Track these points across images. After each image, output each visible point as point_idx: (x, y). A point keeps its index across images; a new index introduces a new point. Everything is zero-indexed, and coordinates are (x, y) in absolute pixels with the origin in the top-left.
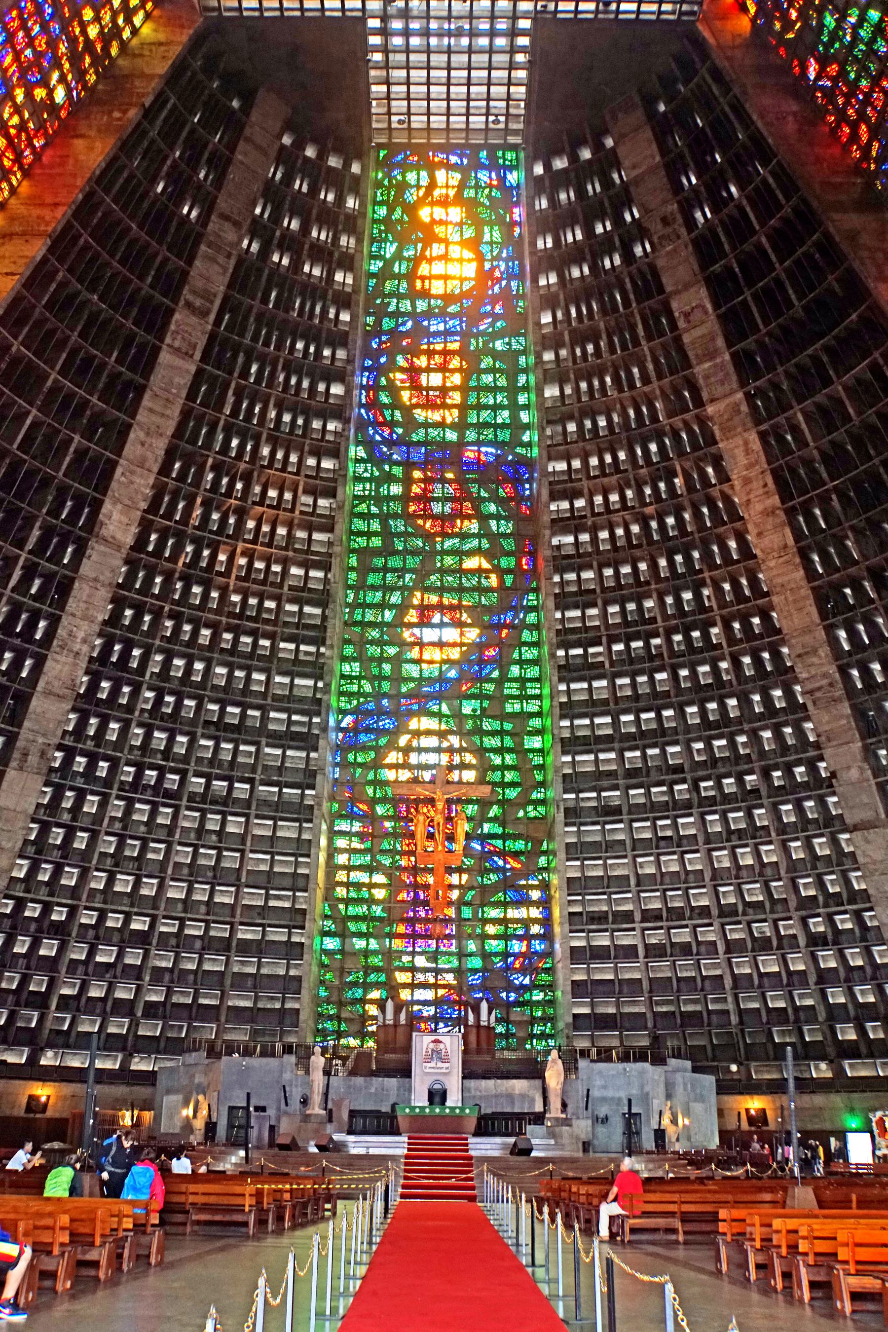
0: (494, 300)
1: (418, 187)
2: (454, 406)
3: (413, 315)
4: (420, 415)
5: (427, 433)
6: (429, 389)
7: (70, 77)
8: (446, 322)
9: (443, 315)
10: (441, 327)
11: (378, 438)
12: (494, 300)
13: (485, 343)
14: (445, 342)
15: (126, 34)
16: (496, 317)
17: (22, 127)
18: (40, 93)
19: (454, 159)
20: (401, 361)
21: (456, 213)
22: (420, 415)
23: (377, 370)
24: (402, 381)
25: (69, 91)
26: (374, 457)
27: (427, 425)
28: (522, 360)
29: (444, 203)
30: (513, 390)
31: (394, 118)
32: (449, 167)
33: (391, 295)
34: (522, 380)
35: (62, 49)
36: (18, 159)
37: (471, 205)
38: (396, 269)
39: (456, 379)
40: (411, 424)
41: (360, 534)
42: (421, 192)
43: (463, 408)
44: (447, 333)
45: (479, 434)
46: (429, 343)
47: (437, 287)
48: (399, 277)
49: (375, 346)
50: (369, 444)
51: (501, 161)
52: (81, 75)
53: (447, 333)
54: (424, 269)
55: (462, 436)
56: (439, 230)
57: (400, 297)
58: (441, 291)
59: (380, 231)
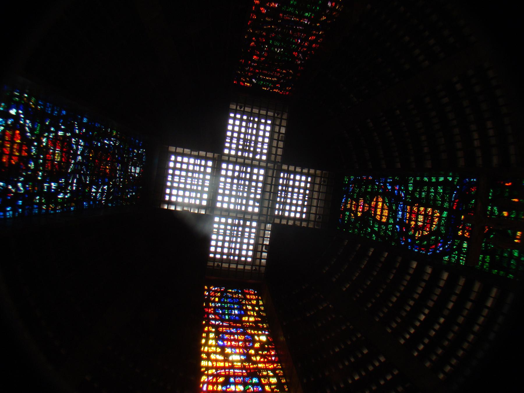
0: (393, 189)
1: (350, 215)
2: (433, 211)
3: (394, 225)
4: (434, 227)
5: (443, 226)
6: (424, 222)
8: (399, 210)
9: (396, 212)
10: (400, 213)
11: (441, 249)
12: (393, 189)
13: (409, 194)
14: (407, 212)
15: (262, 308)
16: (400, 189)
17: (262, 356)
18: (257, 345)
19: (343, 201)
20: (411, 233)
21: (361, 202)
22: (434, 227)
23: (413, 244)
24: (419, 234)
26: (449, 252)
27: (438, 225)
28: (418, 178)
29: (357, 206)
30: (430, 184)
32: (346, 203)
33: (385, 232)
34: (426, 179)
35: (249, 331)
36: (272, 362)
38: (376, 229)
39: (422, 209)
40: (437, 233)
41: (482, 265)
42: (352, 215)
43: (434, 207)
44: (404, 210)
46: (406, 219)
47: (386, 212)
48: (379, 228)
49: (403, 244)
50: (444, 253)
51: (347, 182)
52: (262, 329)
53: (404, 210)
54: (378, 217)
55: (446, 209)
56: (366, 209)
57: (387, 229)
58: (387, 211)
59: (363, 233)
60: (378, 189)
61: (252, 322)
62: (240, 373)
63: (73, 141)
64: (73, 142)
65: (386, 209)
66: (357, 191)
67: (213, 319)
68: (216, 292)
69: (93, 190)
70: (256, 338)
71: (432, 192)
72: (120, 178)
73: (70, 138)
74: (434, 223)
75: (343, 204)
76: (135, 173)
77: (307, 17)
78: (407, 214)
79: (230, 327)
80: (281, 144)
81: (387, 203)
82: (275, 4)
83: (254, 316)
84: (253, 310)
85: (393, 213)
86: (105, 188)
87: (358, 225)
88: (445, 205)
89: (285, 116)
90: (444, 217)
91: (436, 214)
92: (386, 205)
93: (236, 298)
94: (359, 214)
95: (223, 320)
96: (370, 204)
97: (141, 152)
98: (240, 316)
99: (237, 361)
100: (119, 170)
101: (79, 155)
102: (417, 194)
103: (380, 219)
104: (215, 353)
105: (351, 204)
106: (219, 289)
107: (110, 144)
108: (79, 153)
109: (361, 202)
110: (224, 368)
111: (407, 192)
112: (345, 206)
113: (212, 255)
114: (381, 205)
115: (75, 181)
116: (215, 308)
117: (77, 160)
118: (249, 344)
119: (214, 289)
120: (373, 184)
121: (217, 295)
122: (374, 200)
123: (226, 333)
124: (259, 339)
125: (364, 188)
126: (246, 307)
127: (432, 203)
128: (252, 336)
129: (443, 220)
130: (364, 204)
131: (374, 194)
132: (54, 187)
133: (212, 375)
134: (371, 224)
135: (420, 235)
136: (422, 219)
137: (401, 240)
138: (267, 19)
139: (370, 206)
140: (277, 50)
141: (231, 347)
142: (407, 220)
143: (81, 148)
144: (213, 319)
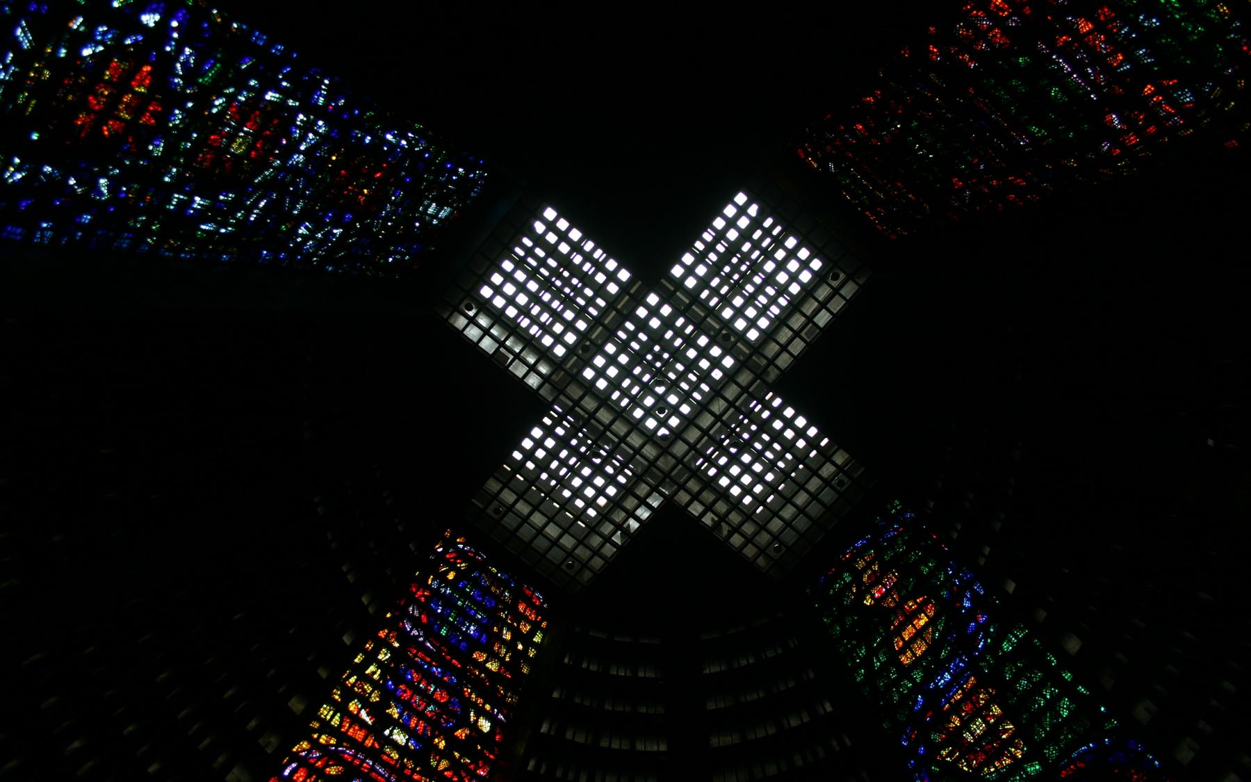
1: (848, 586)
3: (917, 688)
6: (978, 739)
7: (488, 707)
10: (947, 676)
12: (972, 613)
13: (995, 656)
16: (984, 627)
18: (461, 733)
19: (859, 544)
20: (936, 737)
21: (891, 580)
24: (950, 754)
25: (489, 717)
29: (876, 580)
31: (770, 551)
32: (861, 553)
37: (896, 562)
39: (996, 710)
43: (1023, 732)
45: (1056, 743)
46: (948, 701)
47: (920, 649)
52: (497, 702)
56: (890, 603)
57: (897, 683)
60: (943, 586)
61: (488, 671)
62: (383, 776)
63: (299, 119)
64: (298, 123)
65: (926, 643)
66: (900, 548)
67: (412, 619)
68: (462, 555)
69: (302, 231)
70: (472, 714)
71: (1044, 697)
72: (387, 218)
73: (295, 111)
74: (997, 764)
75: (852, 550)
76: (435, 216)
77: (1031, 136)
78: (960, 692)
79: (436, 657)
80: (797, 347)
81: (938, 630)
82: (971, 60)
83: (502, 660)
84: (511, 646)
85: (932, 663)
86: (335, 231)
87: (849, 621)
88: (1049, 749)
89: (849, 290)
90: (1026, 773)
91: (1017, 748)
92: (934, 633)
93: (494, 595)
94: (868, 602)
95: (431, 633)
96: (904, 600)
97: (474, 176)
98: (474, 644)
99: (395, 745)
100: (392, 203)
101: (300, 152)
102: (1011, 670)
103: (900, 649)
104: (365, 703)
105: (868, 565)
106: (472, 552)
107: (398, 145)
108: (303, 148)
109: (891, 580)
110: (358, 746)
111: (994, 647)
112: (853, 560)
113: (517, 455)
114: (922, 623)
115: (262, 204)
116: (436, 594)
117: (290, 162)
118: (447, 721)
119: (461, 546)
120: (941, 566)
121: (459, 565)
122: (918, 600)
123: (418, 668)
124: (476, 721)
125: (917, 554)
126: (501, 630)
127: (1026, 719)
128: (468, 705)
129: (1021, 776)
130: (892, 588)
131: (926, 588)
132: (199, 204)
133: (324, 749)
134: (875, 645)
135: (951, 759)
136: (978, 731)
137: (906, 734)
138: (932, 76)
139: (900, 604)
140: (919, 149)
141: (405, 706)
142: (950, 703)
143: (313, 139)
144: (412, 619)
